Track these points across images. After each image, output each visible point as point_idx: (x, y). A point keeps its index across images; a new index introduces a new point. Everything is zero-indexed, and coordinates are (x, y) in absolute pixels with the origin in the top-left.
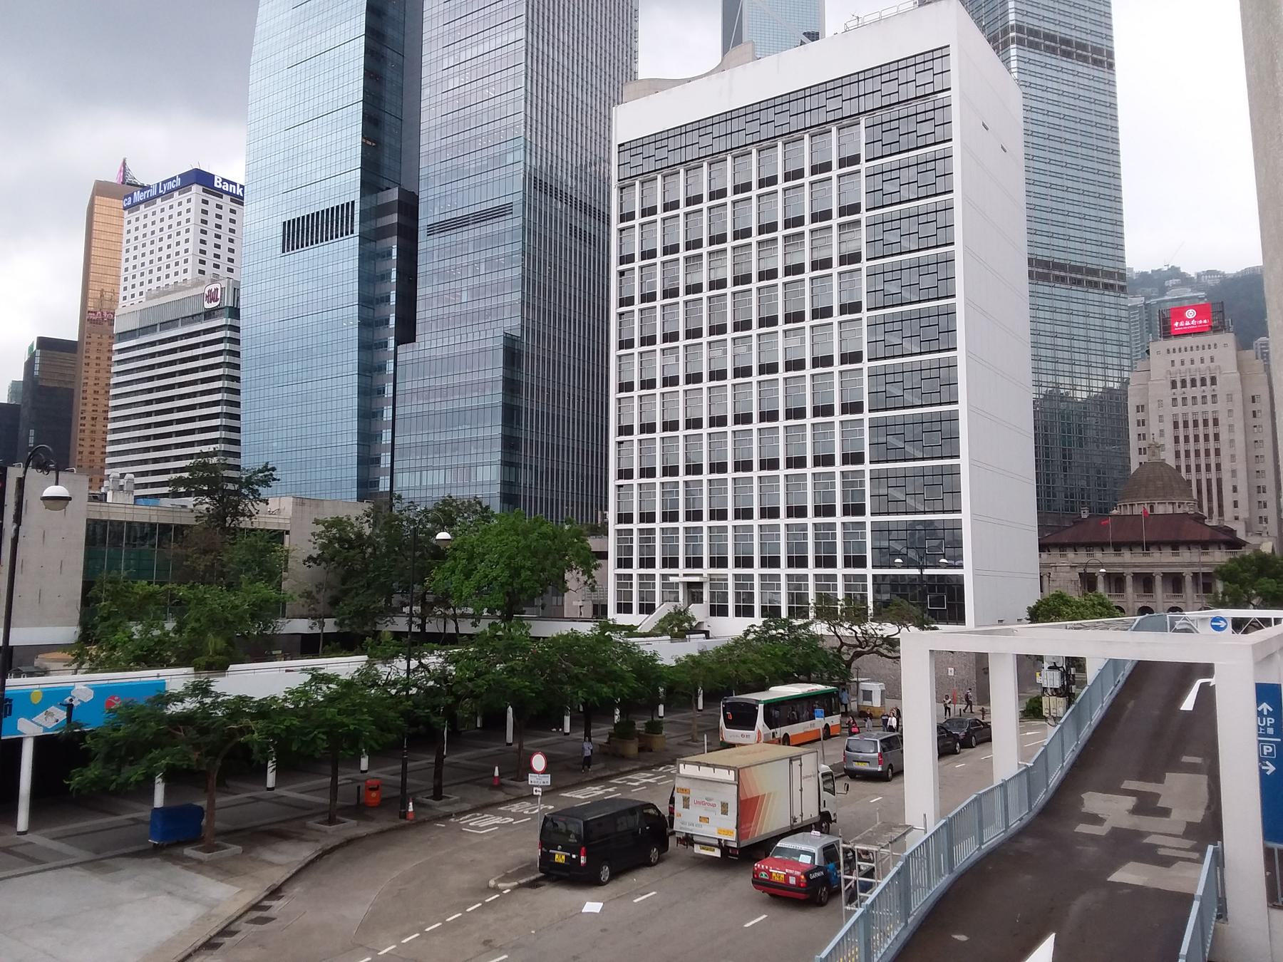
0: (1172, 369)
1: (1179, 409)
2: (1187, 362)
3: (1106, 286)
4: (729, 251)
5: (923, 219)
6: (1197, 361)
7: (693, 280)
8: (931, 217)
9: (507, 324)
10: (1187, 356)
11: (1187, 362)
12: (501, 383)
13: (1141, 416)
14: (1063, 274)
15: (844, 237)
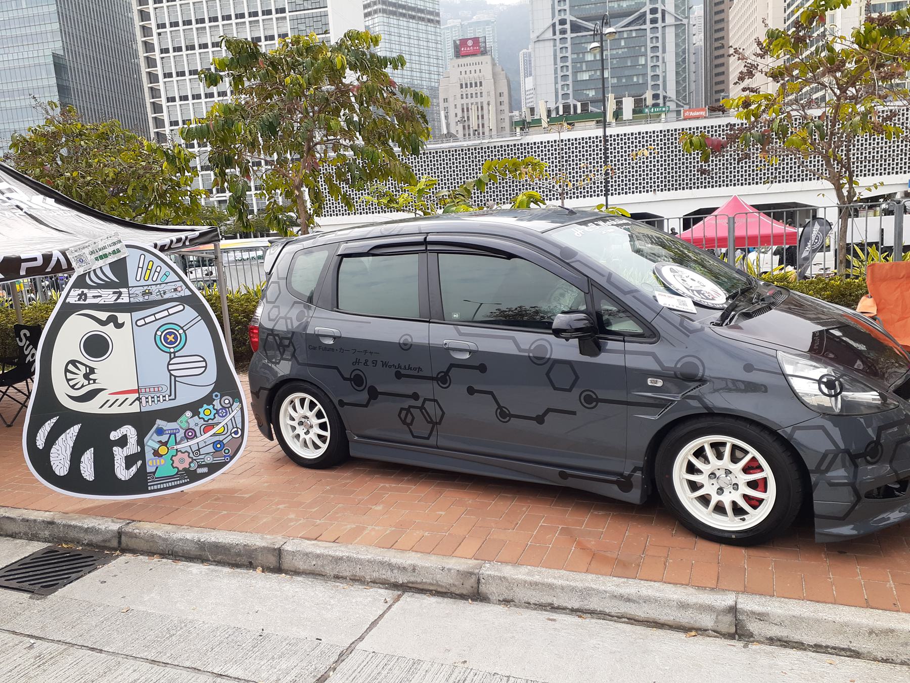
0: (461, 77)
1: (465, 101)
2: (468, 72)
3: (429, 21)
4: (221, 27)
5: (315, 19)
6: (473, 72)
7: (203, 41)
8: (319, 19)
9: (51, 45)
10: (468, 69)
11: (468, 72)
12: (56, 89)
13: (446, 105)
14: (404, 11)
15: (280, 25)
